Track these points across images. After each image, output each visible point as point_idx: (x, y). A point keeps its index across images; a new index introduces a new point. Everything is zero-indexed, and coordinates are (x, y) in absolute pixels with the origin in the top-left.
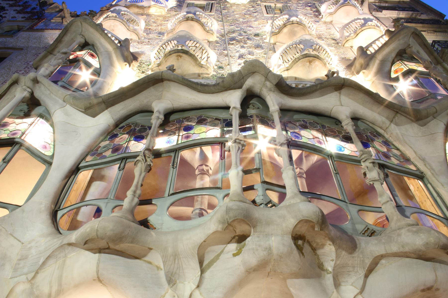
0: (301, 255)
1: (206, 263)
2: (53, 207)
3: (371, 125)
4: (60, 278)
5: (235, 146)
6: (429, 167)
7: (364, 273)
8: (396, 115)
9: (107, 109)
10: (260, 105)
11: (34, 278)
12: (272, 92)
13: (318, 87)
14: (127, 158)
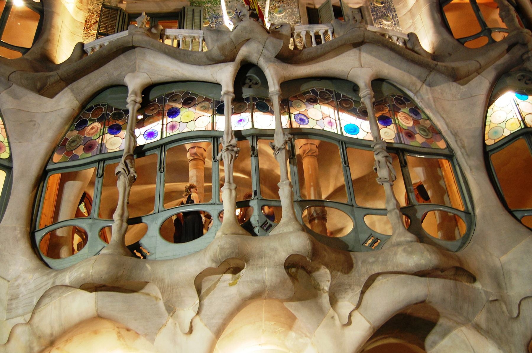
0: (295, 281)
2: (28, 229)
3: (398, 86)
5: (228, 155)
6: (460, 145)
7: (360, 290)
8: (431, 71)
9: (67, 86)
10: (258, 78)
11: (31, 319)
12: (272, 64)
14: (105, 160)
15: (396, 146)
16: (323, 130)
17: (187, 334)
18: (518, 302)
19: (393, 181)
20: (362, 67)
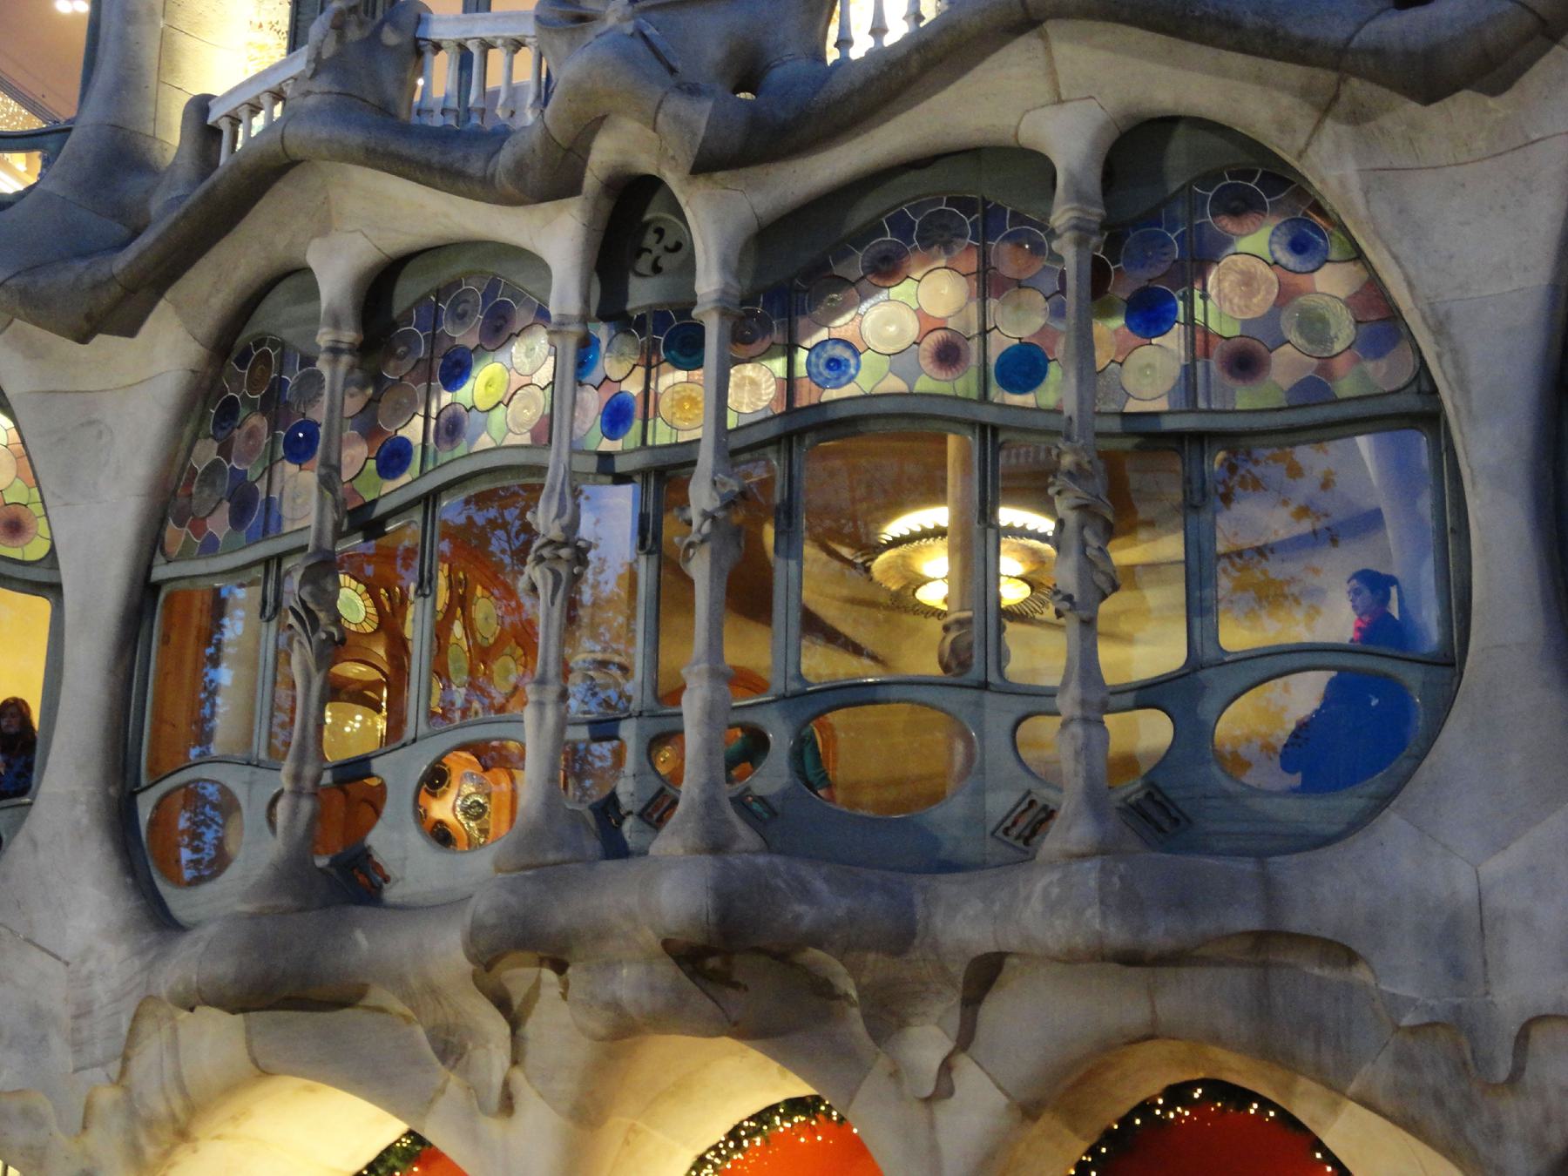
0: (729, 991)
1: (517, 1001)
4: (178, 1078)
5: (544, 578)
13: (914, 68)
15: (1169, 424)
16: (911, 394)
17: (494, 1116)
18: (1515, 1029)
19: (1104, 597)
20: (1060, 101)
